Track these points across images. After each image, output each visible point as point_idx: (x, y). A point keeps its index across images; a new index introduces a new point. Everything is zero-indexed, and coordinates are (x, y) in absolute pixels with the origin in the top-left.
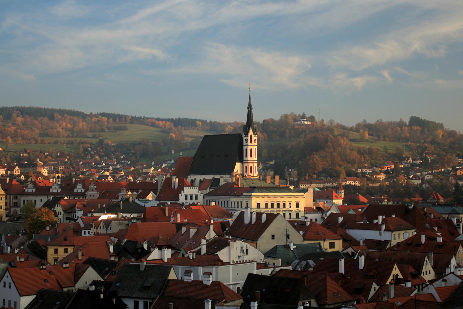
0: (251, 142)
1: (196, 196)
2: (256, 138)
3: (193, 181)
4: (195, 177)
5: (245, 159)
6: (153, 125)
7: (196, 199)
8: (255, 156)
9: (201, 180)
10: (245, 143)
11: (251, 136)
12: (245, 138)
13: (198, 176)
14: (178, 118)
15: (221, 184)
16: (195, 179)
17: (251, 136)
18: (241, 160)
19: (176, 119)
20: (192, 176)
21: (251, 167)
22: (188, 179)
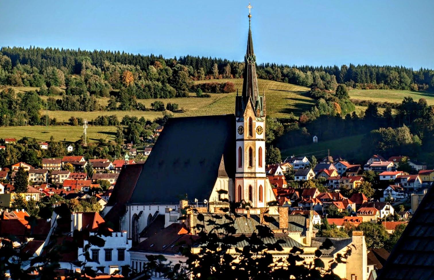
0: (251, 134)
1: (121, 252)
2: (262, 125)
3: (136, 217)
4: (141, 208)
5: (238, 170)
6: (294, 80)
7: (121, 257)
8: (260, 165)
9: (150, 215)
10: (238, 136)
11: (251, 120)
12: (238, 125)
13: (147, 207)
14: (333, 66)
15: (166, 226)
16: (141, 212)
17: (251, 120)
18: (231, 173)
19: (344, 67)
20: (135, 207)
21: (250, 188)
22: (128, 214)
